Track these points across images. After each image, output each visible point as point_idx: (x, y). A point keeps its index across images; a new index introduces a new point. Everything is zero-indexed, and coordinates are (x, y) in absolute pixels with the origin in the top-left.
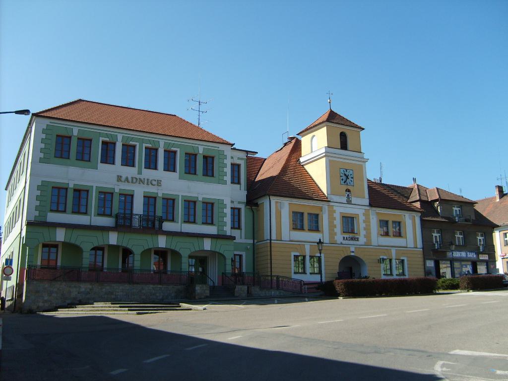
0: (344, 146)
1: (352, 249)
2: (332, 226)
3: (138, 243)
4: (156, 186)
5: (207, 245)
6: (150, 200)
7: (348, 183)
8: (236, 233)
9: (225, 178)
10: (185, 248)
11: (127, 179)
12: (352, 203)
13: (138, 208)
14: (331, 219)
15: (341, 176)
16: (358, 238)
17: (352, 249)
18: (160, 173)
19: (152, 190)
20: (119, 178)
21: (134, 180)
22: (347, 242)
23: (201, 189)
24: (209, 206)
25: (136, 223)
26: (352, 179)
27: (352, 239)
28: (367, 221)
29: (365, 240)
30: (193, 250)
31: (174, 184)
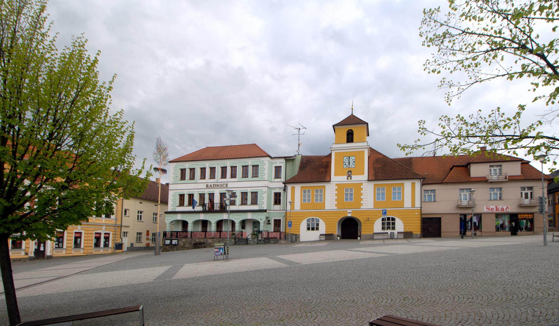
3: (213, 218)
5: (249, 216)
6: (222, 195)
13: (217, 200)
20: (207, 186)
25: (217, 207)
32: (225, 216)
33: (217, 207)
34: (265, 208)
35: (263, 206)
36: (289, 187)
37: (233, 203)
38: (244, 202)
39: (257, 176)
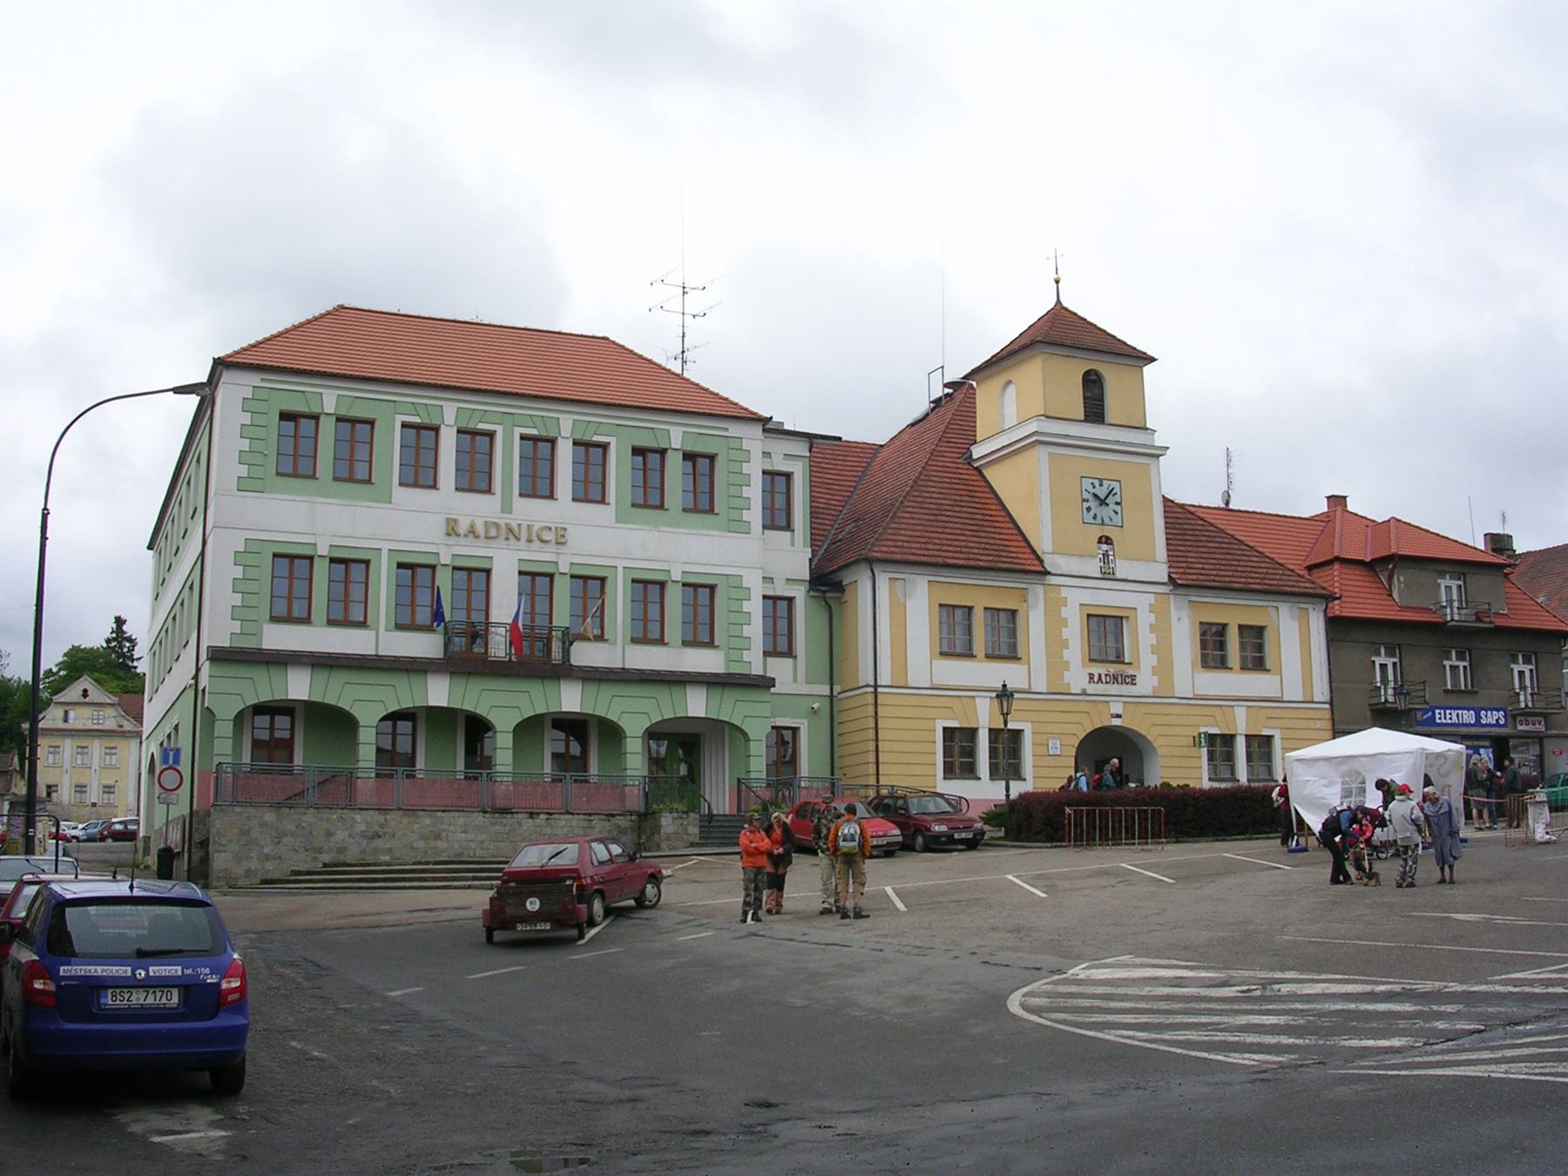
0: (1095, 411)
1: (1115, 711)
2: (1055, 644)
3: (505, 706)
4: (552, 548)
5: (697, 704)
6: (535, 580)
7: (1106, 520)
8: (780, 669)
9: (746, 515)
10: (635, 714)
11: (472, 531)
12: (1118, 576)
13: (505, 604)
14: (1055, 624)
16: (1133, 677)
17: (1116, 708)
18: (562, 509)
19: (541, 556)
20: (451, 529)
22: (1101, 688)
23: (679, 548)
24: (702, 592)
25: (499, 647)
26: (1118, 508)
27: (1115, 679)
28: (1162, 629)
29: (1155, 681)
30: (657, 718)
31: (608, 538)
35: (746, 656)
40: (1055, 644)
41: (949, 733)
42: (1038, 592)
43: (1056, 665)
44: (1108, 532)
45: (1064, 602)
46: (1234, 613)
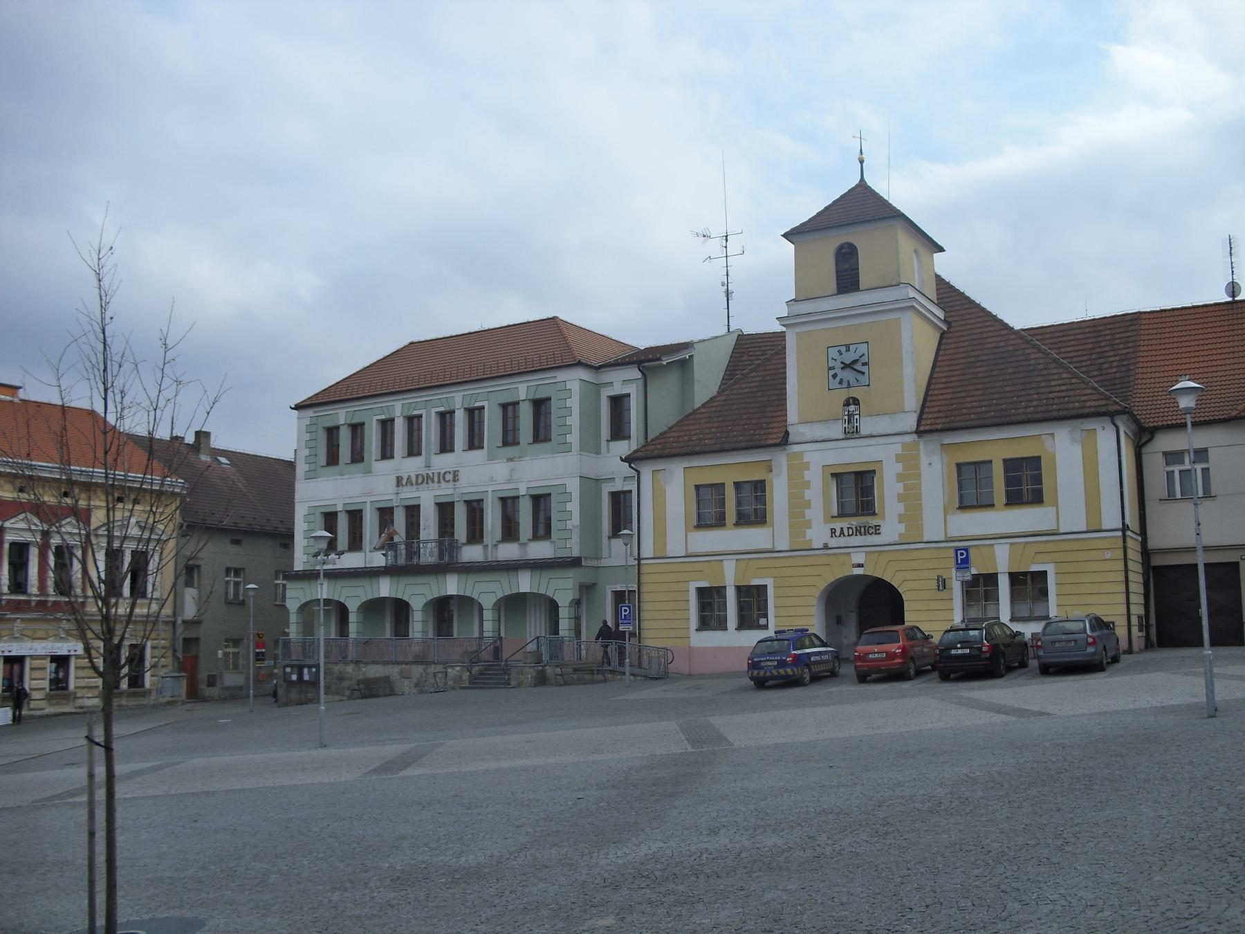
0: (848, 281)
1: (859, 559)
2: (798, 505)
3: (418, 594)
4: (451, 485)
5: (524, 583)
6: (445, 510)
14: (797, 485)
15: (830, 369)
17: (858, 558)
18: (460, 458)
19: (445, 491)
21: (420, 480)
22: (843, 541)
23: (534, 470)
25: (428, 555)
27: (858, 531)
28: (910, 476)
29: (901, 528)
32: (452, 586)
33: (428, 555)
34: (576, 553)
36: (647, 471)
37: (475, 534)
38: (510, 531)
39: (548, 439)
40: (798, 505)
41: (701, 592)
42: (781, 459)
43: (798, 522)
44: (854, 393)
45: (806, 466)
46: (996, 446)
